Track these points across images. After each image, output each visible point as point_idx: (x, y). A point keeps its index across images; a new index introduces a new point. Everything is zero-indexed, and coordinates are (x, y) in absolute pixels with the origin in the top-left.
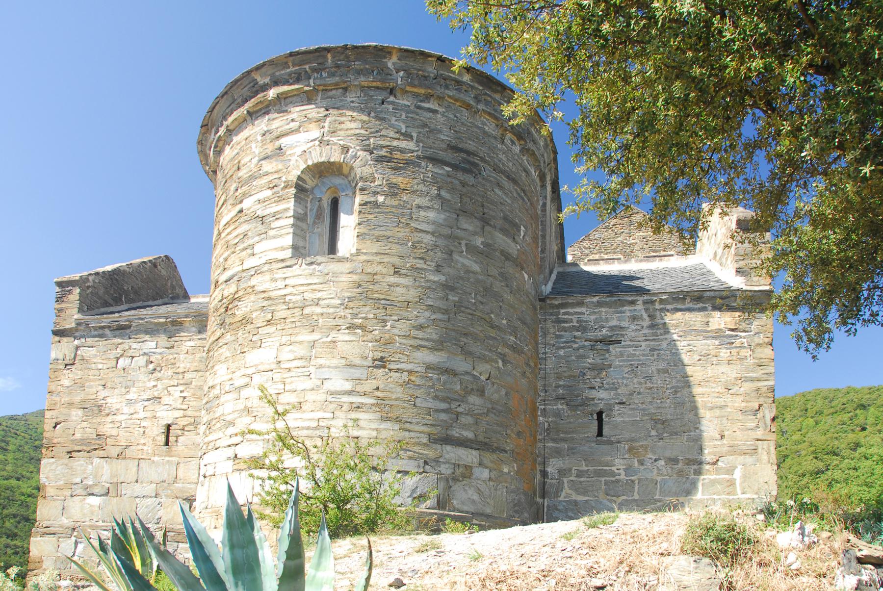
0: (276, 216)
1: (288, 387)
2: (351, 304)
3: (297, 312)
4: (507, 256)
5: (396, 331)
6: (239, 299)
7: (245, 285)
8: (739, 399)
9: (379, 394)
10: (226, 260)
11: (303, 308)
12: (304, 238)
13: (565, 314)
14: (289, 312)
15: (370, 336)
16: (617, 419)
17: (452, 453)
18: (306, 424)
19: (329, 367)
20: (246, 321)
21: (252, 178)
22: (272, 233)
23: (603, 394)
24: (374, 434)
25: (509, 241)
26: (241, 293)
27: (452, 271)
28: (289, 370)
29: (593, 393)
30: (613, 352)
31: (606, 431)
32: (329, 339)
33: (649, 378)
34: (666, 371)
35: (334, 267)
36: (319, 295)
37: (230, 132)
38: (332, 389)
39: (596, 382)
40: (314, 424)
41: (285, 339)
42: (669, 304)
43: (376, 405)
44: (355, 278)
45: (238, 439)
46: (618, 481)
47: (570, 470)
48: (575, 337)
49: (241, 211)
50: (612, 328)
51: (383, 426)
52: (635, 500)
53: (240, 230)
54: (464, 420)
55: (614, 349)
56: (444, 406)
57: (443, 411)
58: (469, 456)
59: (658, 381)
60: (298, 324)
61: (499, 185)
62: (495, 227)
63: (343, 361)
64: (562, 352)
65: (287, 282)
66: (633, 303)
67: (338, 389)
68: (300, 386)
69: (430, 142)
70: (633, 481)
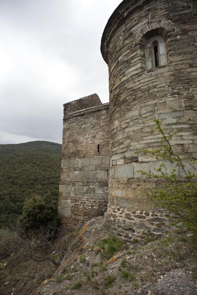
0: (133, 58)
2: (171, 84)
3: (146, 93)
5: (195, 92)
7: (123, 88)
11: (149, 91)
14: (143, 93)
15: (182, 96)
18: (156, 141)
19: (164, 113)
20: (125, 101)
24: (191, 142)
26: (121, 92)
28: (146, 117)
32: (162, 101)
35: (160, 71)
36: (155, 84)
38: (167, 123)
41: (142, 105)
43: (190, 128)
44: (171, 73)
45: (125, 150)
49: (118, 62)
53: (118, 69)
60: (147, 98)
63: (171, 110)
65: (140, 82)
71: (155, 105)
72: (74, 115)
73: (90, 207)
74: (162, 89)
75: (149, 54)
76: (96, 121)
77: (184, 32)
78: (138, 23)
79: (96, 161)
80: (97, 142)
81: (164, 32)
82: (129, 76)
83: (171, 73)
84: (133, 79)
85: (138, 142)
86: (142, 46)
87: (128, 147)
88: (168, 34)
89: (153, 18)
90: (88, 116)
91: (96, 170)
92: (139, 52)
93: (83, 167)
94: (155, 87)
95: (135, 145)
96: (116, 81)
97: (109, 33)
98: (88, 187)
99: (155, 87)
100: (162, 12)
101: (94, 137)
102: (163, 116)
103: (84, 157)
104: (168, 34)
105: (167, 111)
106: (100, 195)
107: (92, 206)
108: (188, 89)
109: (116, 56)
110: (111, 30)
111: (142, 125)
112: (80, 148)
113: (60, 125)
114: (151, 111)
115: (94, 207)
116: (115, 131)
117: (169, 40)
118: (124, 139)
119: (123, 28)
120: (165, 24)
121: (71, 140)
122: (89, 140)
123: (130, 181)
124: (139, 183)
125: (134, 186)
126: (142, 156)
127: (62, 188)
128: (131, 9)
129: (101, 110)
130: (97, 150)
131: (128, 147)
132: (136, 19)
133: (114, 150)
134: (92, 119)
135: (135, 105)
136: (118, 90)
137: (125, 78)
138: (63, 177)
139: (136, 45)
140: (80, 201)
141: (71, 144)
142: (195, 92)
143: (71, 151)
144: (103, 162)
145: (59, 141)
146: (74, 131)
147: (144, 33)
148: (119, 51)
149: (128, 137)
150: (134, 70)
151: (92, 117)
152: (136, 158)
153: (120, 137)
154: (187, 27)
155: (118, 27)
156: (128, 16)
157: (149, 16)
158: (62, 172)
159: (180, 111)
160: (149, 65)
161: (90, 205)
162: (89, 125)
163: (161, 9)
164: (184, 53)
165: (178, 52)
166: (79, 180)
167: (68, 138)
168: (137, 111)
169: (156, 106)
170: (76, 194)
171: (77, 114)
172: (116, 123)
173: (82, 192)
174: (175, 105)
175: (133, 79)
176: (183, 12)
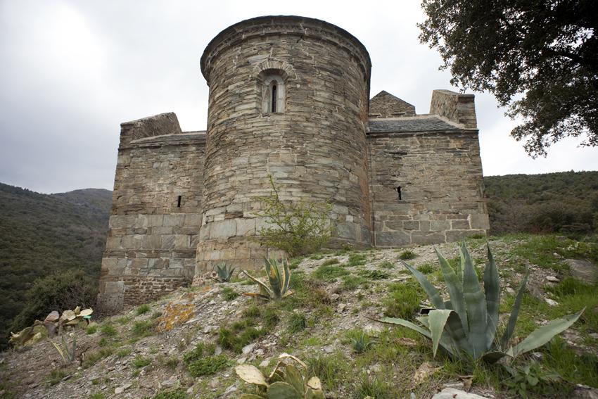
0: (247, 93)
1: (255, 176)
2: (286, 136)
4: (355, 113)
5: (308, 148)
6: (227, 133)
8: (467, 182)
9: (301, 179)
10: (219, 114)
11: (262, 137)
12: (261, 104)
13: (379, 140)
16: (408, 190)
17: (336, 208)
20: (232, 143)
21: (234, 75)
22: (245, 101)
23: (399, 179)
24: (299, 199)
25: (355, 106)
26: (228, 130)
27: (333, 120)
28: (256, 167)
29: (395, 178)
30: (403, 159)
31: (402, 196)
33: (422, 171)
34: (430, 168)
35: (277, 118)
36: (270, 131)
37: (220, 53)
39: (396, 173)
40: (269, 195)
42: (429, 136)
43: (300, 185)
44: (288, 123)
45: (227, 203)
46: (410, 222)
47: (386, 216)
48: (385, 152)
49: (228, 91)
50: (402, 148)
51: (304, 195)
52: (420, 232)
53: (226, 101)
54: (340, 191)
55: (404, 158)
56: (332, 185)
57: (332, 187)
58: (345, 210)
59: (426, 173)
61: (351, 81)
62: (349, 100)
64: (378, 159)
65: (254, 125)
66: (412, 136)
67: (281, 177)
68: (262, 175)
69: (320, 60)
70: (418, 222)
71: (267, 155)
72: (141, 145)
73: (159, 290)
74: (276, 138)
75: (267, 94)
76: (178, 159)
77: (305, 83)
78: (257, 54)
79: (174, 220)
80: (178, 191)
81: (284, 75)
82: (241, 114)
83: (288, 123)
84: (245, 120)
85: (244, 194)
86: (260, 83)
87: (231, 200)
88: (288, 79)
89: (275, 55)
90: (166, 150)
91: (173, 233)
92: (255, 88)
93: (150, 228)
94: (269, 135)
95: (240, 198)
96: (221, 115)
97: (219, 46)
98: (157, 259)
99: (269, 135)
100: (284, 52)
101: (174, 184)
102: (274, 169)
103: (153, 213)
104: (288, 79)
105: (279, 163)
106: (178, 270)
107: (162, 288)
108: (302, 144)
109: (224, 81)
110: (222, 44)
111: (251, 176)
112: (147, 199)
113: (113, 159)
114: (262, 162)
115: (167, 290)
116: (215, 178)
117: (289, 86)
118: (227, 190)
119: (238, 50)
120: (286, 66)
121: (131, 184)
122: (165, 187)
123: (231, 239)
124: (242, 242)
125: (236, 244)
126: (248, 210)
127: (107, 263)
128: (250, 34)
129: (187, 145)
130: (177, 203)
131: (231, 200)
132: (255, 47)
133: (211, 202)
134: (173, 155)
135: (244, 150)
136: (224, 128)
137: (234, 115)
138: (112, 244)
139: (252, 79)
140: (142, 282)
141: (130, 192)
142: (308, 148)
143: (131, 203)
144: (186, 222)
145: (110, 187)
146: (139, 170)
147: (264, 69)
148: (230, 77)
149: (233, 188)
150: (247, 109)
151: (173, 153)
152: (241, 213)
153: (221, 187)
154: (307, 77)
155: (233, 45)
156: (245, 40)
157: (271, 51)
158: (110, 236)
159: (292, 166)
160: (266, 107)
161: (160, 286)
162: (166, 164)
163: (284, 49)
164: (302, 104)
165: (297, 102)
166: (141, 249)
167: (126, 182)
168: (247, 159)
169: (268, 156)
170: (135, 271)
171: (147, 145)
172: (218, 168)
173: (146, 267)
174: (288, 160)
175: (245, 120)
176: (304, 61)
